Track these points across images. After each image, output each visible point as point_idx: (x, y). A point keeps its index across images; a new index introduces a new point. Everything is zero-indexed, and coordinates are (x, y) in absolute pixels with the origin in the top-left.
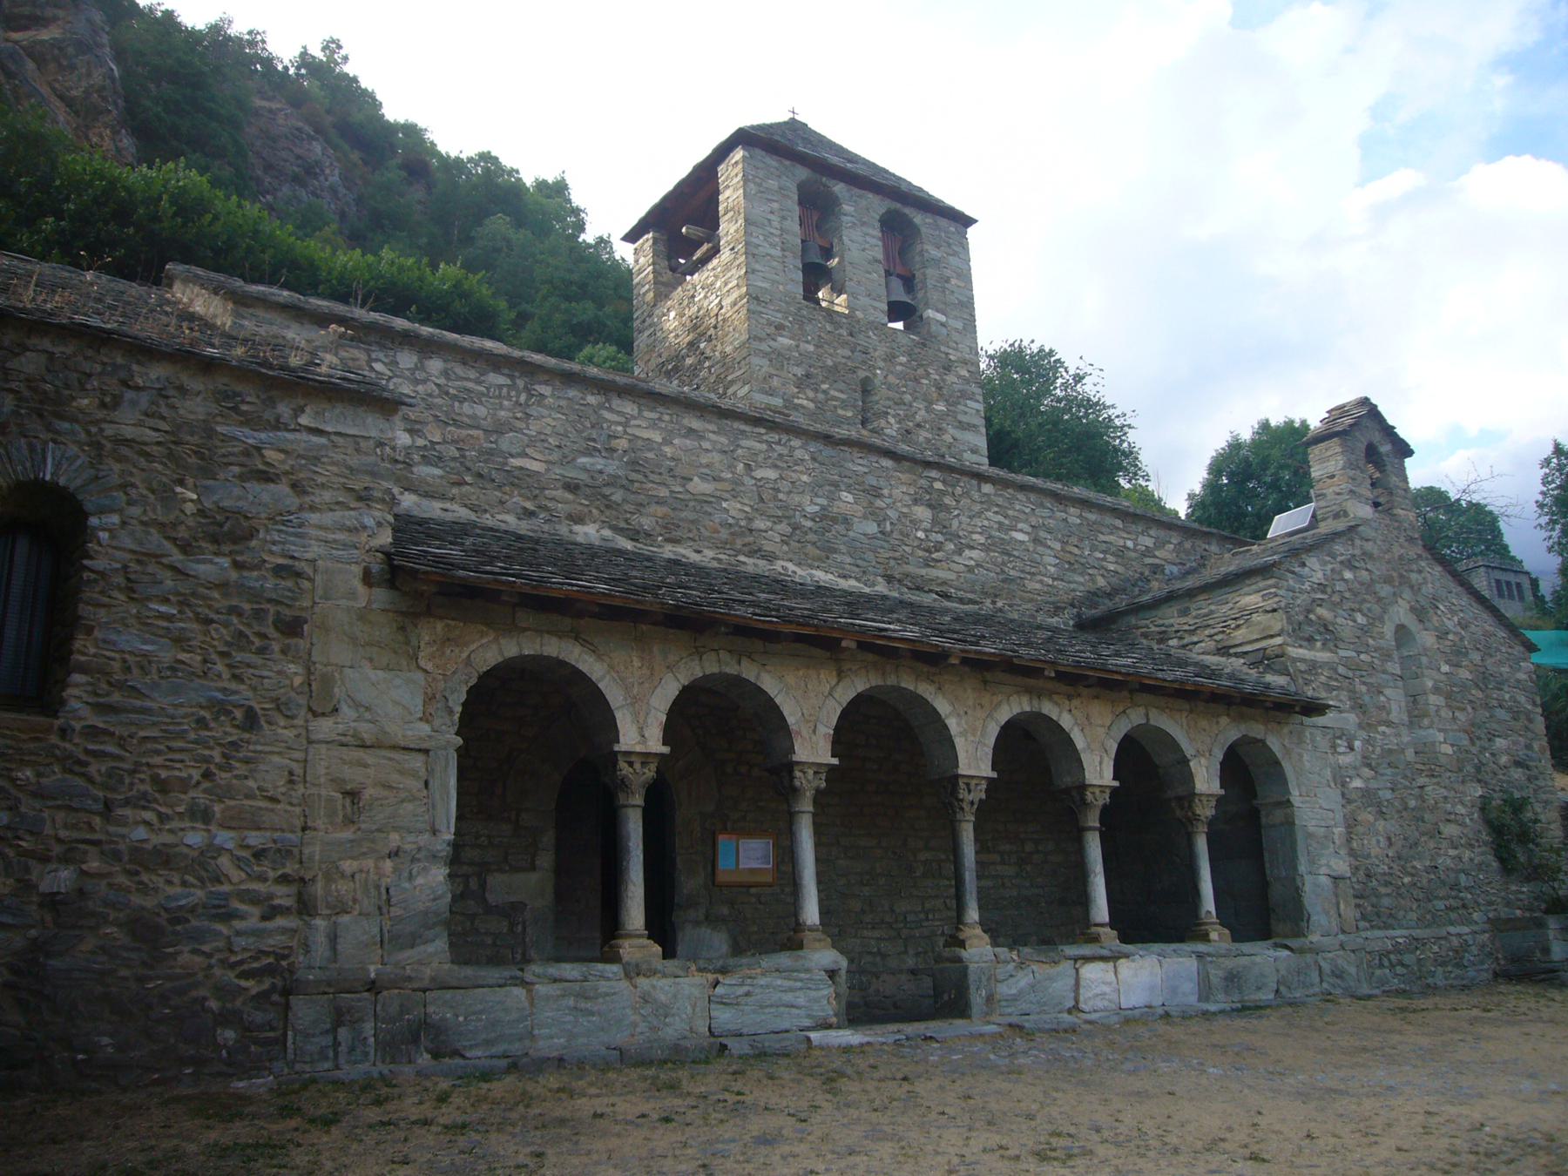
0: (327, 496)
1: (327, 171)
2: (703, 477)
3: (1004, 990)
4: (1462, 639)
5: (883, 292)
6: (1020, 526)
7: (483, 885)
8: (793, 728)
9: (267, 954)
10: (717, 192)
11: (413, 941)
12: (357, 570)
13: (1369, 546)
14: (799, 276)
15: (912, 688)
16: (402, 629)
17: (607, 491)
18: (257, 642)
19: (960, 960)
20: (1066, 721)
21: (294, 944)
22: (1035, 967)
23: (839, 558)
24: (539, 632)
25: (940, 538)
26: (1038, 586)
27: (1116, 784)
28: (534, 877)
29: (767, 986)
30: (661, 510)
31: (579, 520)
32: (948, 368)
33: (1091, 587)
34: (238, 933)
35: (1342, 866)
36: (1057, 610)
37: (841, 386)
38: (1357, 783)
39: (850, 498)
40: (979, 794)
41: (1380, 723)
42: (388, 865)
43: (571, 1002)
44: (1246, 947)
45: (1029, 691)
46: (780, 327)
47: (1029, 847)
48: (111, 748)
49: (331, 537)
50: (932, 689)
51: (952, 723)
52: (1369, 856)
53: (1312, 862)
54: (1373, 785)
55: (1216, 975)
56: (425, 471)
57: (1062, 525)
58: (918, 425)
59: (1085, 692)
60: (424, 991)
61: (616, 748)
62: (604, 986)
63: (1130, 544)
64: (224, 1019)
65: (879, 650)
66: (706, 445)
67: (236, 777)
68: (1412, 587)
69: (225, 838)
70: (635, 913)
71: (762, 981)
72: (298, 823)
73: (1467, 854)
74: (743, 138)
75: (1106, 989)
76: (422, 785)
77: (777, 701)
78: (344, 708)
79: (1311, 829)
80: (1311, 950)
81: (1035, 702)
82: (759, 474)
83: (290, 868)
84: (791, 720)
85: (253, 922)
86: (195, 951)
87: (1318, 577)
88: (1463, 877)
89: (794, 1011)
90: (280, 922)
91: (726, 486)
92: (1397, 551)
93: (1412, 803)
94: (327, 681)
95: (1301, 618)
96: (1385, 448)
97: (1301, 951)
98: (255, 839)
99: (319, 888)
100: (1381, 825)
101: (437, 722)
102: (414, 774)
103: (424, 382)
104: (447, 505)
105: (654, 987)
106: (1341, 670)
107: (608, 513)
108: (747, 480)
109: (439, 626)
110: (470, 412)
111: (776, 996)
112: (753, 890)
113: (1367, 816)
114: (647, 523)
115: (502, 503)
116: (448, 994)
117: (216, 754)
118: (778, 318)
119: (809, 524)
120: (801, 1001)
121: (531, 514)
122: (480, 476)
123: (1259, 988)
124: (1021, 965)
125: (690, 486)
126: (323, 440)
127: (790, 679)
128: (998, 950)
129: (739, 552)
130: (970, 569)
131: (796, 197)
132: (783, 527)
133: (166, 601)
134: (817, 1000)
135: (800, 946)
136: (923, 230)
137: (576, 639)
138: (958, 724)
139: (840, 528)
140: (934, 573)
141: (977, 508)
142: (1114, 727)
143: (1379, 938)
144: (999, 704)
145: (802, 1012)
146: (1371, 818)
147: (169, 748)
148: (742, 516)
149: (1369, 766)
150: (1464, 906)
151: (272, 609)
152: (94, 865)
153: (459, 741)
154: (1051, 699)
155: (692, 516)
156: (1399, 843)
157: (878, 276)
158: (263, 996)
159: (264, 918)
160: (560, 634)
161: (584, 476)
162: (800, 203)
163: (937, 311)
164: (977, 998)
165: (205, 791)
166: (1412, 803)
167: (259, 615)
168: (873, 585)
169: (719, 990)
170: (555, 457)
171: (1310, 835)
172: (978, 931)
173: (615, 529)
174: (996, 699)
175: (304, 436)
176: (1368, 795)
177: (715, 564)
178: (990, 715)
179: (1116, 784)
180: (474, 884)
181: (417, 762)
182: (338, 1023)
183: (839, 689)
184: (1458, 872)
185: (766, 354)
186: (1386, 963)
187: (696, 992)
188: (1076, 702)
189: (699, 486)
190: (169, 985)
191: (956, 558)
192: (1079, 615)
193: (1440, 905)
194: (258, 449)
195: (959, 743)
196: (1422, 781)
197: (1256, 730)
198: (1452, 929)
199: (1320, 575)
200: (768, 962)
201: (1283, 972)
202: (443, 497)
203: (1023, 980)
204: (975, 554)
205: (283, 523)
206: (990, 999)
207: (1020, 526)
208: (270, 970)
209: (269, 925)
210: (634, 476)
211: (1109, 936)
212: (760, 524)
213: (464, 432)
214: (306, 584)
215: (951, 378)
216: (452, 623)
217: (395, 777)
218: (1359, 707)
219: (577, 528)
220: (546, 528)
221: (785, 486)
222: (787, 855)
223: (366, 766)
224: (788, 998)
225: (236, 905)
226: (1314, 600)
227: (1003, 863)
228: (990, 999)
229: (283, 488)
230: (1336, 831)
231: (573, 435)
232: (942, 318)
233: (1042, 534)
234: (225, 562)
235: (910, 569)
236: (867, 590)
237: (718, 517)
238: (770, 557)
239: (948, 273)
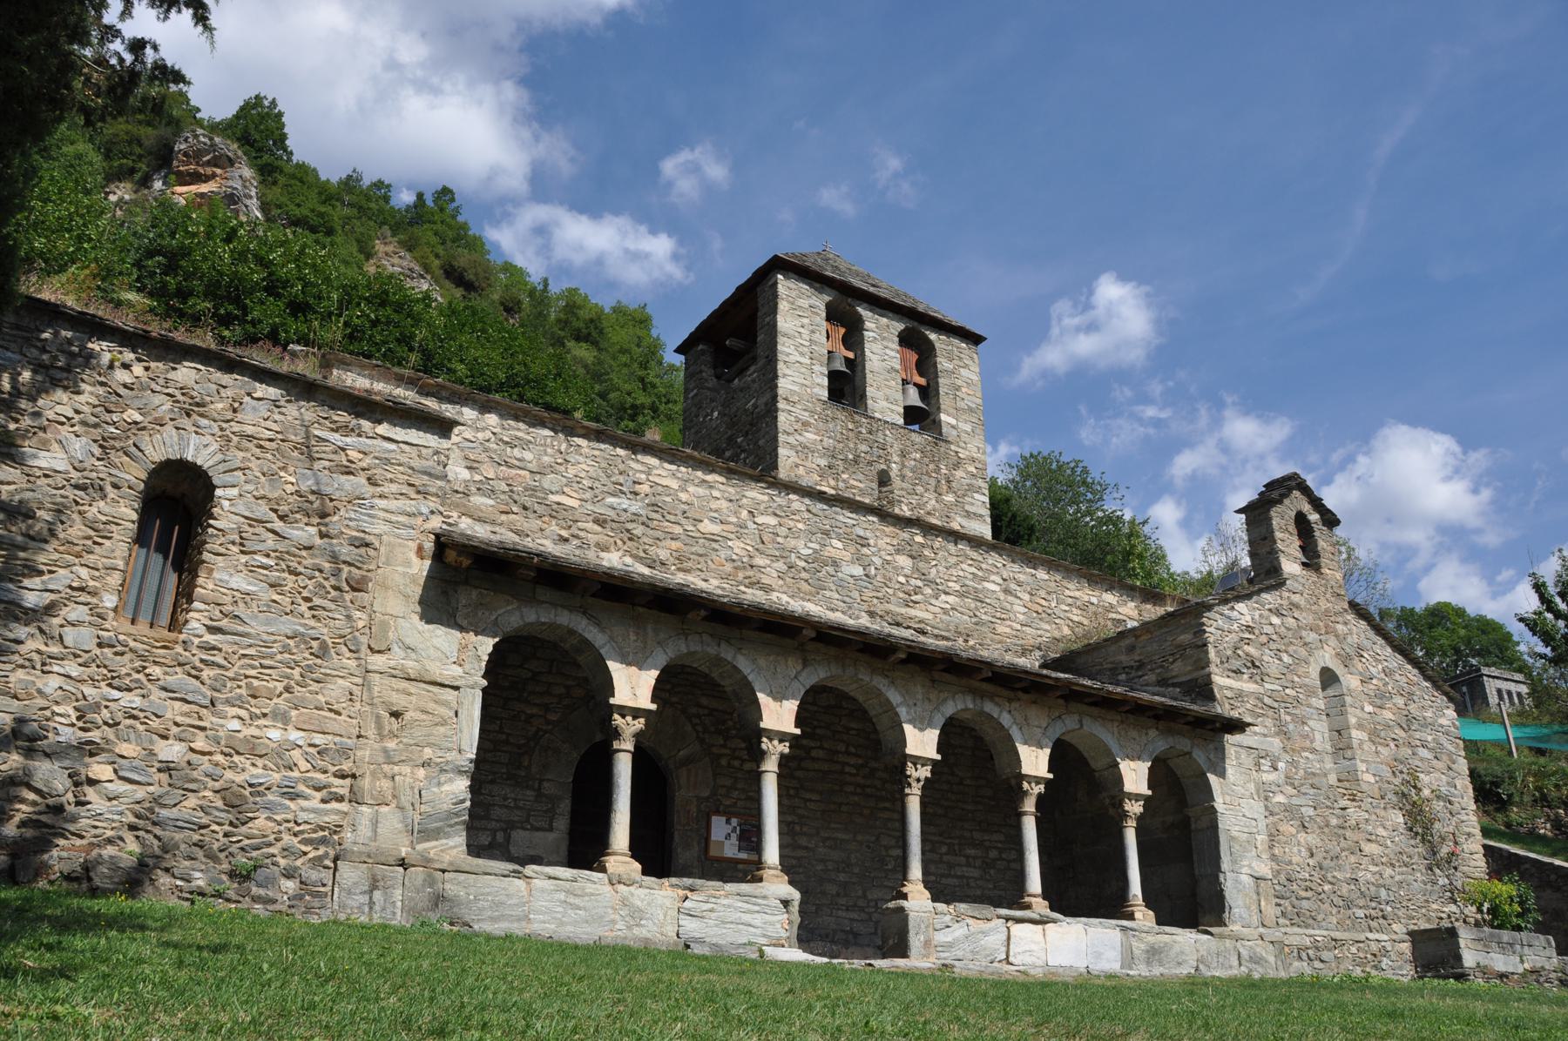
0: (394, 488)
2: (713, 520)
3: (941, 937)
4: (1386, 684)
5: (899, 396)
6: (993, 578)
7: (508, 839)
9: (323, 829)
10: (757, 310)
11: (435, 834)
12: (413, 545)
13: (1296, 598)
14: (825, 382)
16: (445, 593)
17: (629, 526)
18: (334, 593)
19: (902, 909)
20: (1006, 720)
21: (344, 823)
22: (970, 921)
23: (828, 594)
24: (554, 605)
25: (920, 583)
26: (1008, 630)
27: (1051, 776)
28: (551, 836)
30: (675, 545)
31: (605, 549)
32: (957, 466)
33: (1057, 634)
34: (303, 810)
35: (1264, 869)
36: (1024, 652)
37: (861, 477)
38: (1280, 798)
39: (840, 545)
40: (925, 772)
41: (1304, 749)
42: (421, 773)
43: (562, 896)
44: (1168, 929)
45: (974, 692)
46: (806, 424)
47: (993, 854)
48: (219, 659)
49: (394, 518)
50: (885, 681)
52: (1290, 863)
53: (1234, 862)
54: (1295, 801)
55: (1139, 947)
56: (478, 500)
57: (1030, 580)
59: (1025, 697)
60: (444, 871)
61: (612, 701)
62: (590, 888)
63: (1094, 600)
64: (289, 874)
66: (716, 493)
67: (310, 692)
68: (1337, 636)
69: (294, 735)
70: (620, 834)
71: (725, 902)
72: (355, 732)
73: (1388, 871)
74: (777, 265)
76: (452, 714)
77: (750, 678)
78: (395, 648)
79: (1234, 834)
80: (1230, 937)
81: (978, 701)
82: (760, 520)
83: (346, 766)
85: (315, 803)
86: (268, 818)
87: (1247, 619)
88: (1383, 893)
90: (335, 805)
91: (731, 528)
92: (1324, 604)
93: (1334, 821)
94: (384, 626)
95: (1229, 653)
96: (1314, 517)
97: (1221, 937)
98: (319, 739)
99: (366, 783)
100: (1302, 836)
101: (467, 667)
102: (445, 704)
103: (483, 429)
104: (497, 529)
106: (1267, 700)
107: (629, 543)
108: (751, 525)
109: (474, 594)
110: (519, 456)
112: (740, 866)
113: (1288, 828)
114: (663, 554)
116: (462, 877)
117: (296, 672)
118: (805, 416)
119: (803, 564)
120: (757, 922)
122: (525, 508)
123: (1179, 964)
124: (958, 918)
125: (701, 526)
126: (393, 446)
127: (762, 662)
128: (937, 905)
129: (741, 583)
130: (945, 611)
131: (824, 315)
132: (781, 565)
133: (268, 556)
134: (772, 924)
135: (761, 880)
136: (937, 345)
137: (584, 613)
139: (831, 569)
140: (912, 612)
141: (953, 560)
142: (1051, 729)
143: (1298, 936)
144: (945, 700)
145: (758, 931)
146: (1294, 831)
147: (262, 666)
148: (744, 553)
149: (1292, 785)
150: (1384, 917)
151: (346, 569)
152: (200, 744)
153: (485, 683)
154: (992, 700)
155: (701, 551)
156: (1319, 856)
157: (896, 384)
158: (317, 862)
159: (324, 801)
160: (571, 609)
161: (612, 514)
162: (828, 319)
164: (915, 941)
165: (285, 700)
166: (1334, 821)
167: (336, 573)
168: (858, 618)
169: (687, 904)
170: (588, 495)
171: (1233, 838)
172: (921, 886)
174: (942, 696)
175: (379, 442)
176: (1290, 811)
177: (720, 592)
178: (937, 708)
179: (1051, 776)
180: (500, 837)
181: (449, 695)
182: (374, 887)
184: (1378, 886)
185: (792, 447)
186: (1304, 955)
187: (668, 903)
188: (1015, 705)
189: (708, 527)
190: (247, 842)
191: (933, 601)
192: (1043, 657)
193: (1360, 913)
194: (343, 450)
196: (1344, 803)
197: (1183, 744)
198: (1371, 936)
199: (1248, 618)
200: (730, 887)
202: (493, 523)
203: (959, 931)
204: (951, 599)
205: (360, 506)
207: (993, 578)
208: (323, 841)
209: (328, 806)
210: (654, 516)
211: (1040, 906)
212: (760, 561)
213: (514, 472)
214: (371, 552)
215: (959, 473)
217: (431, 706)
218: (1282, 732)
219: (603, 554)
220: (577, 552)
221: (783, 531)
223: (410, 694)
224: (747, 918)
225: (301, 788)
226: (1242, 639)
227: (968, 865)
228: (927, 943)
229: (361, 480)
230: (1259, 838)
231: (604, 480)
232: (953, 422)
233: (1013, 586)
234: (313, 530)
235: (891, 607)
236: (851, 622)
237: (723, 554)
238: (767, 589)
239: (959, 382)
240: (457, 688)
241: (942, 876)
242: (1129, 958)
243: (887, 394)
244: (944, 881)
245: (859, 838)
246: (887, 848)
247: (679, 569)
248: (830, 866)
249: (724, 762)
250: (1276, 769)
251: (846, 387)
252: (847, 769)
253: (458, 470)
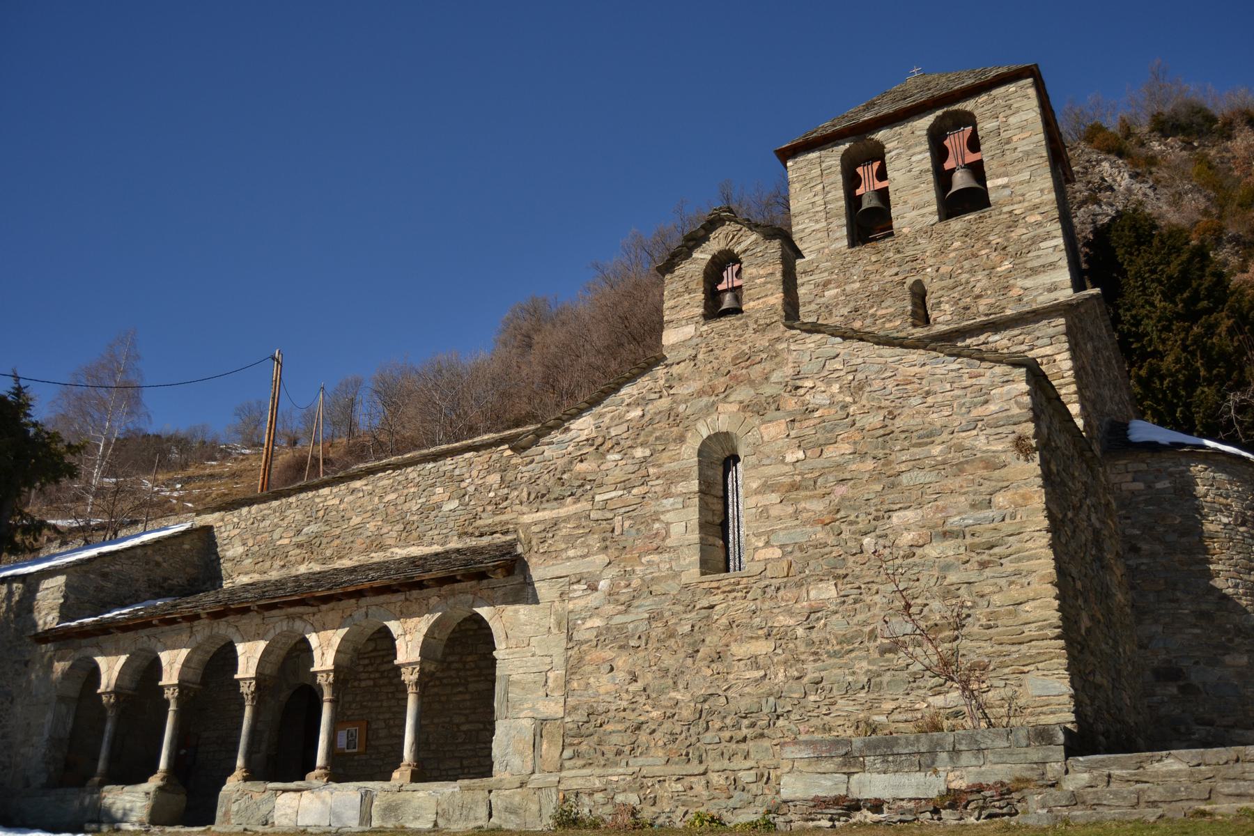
1: (1119, 179)
25: (506, 491)
30: (337, 542)
58: (979, 297)
75: (289, 811)
82: (386, 500)
123: (416, 818)
125: (353, 522)
163: (998, 177)
189: (356, 520)
201: (445, 806)
242: (366, 817)
243: (913, 201)
246: (458, 725)
250: (595, 589)
251: (868, 222)
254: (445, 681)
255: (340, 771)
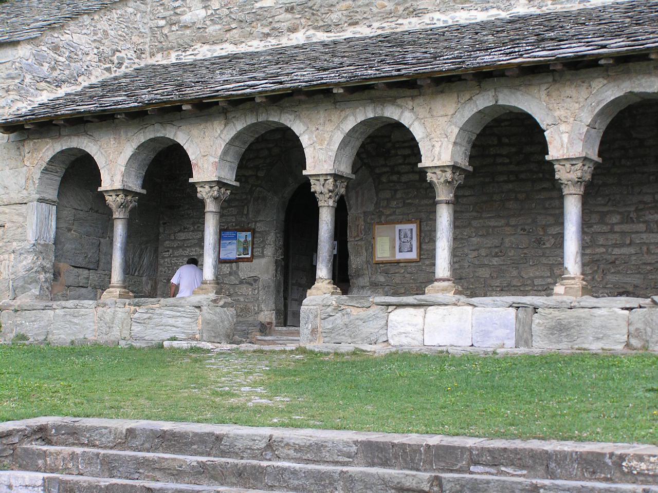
8: (193, 162)
15: (276, 120)
16: (19, 148)
28: (263, 261)
29: (161, 314)
50: (292, 117)
51: (305, 140)
56: (212, 29)
62: (83, 311)
65: (238, 104)
75: (409, 329)
84: (192, 157)
89: (174, 329)
105: (105, 313)
111: (164, 320)
114: (334, 17)
115: (251, 34)
121: (268, 35)
129: (400, 17)
138: (309, 139)
144: (346, 117)
169: (136, 315)
173: (317, 28)
183: (225, 132)
195: (308, 153)
206: (314, 331)
216: (36, 141)
222: (427, 239)
240: (25, 203)
241: (615, 246)
244: (616, 251)
245: (513, 222)
247: (350, 25)
248: (483, 252)
249: (384, 179)
252: (499, 160)
253: (197, 12)
254: (523, 176)
255: (470, 284)
